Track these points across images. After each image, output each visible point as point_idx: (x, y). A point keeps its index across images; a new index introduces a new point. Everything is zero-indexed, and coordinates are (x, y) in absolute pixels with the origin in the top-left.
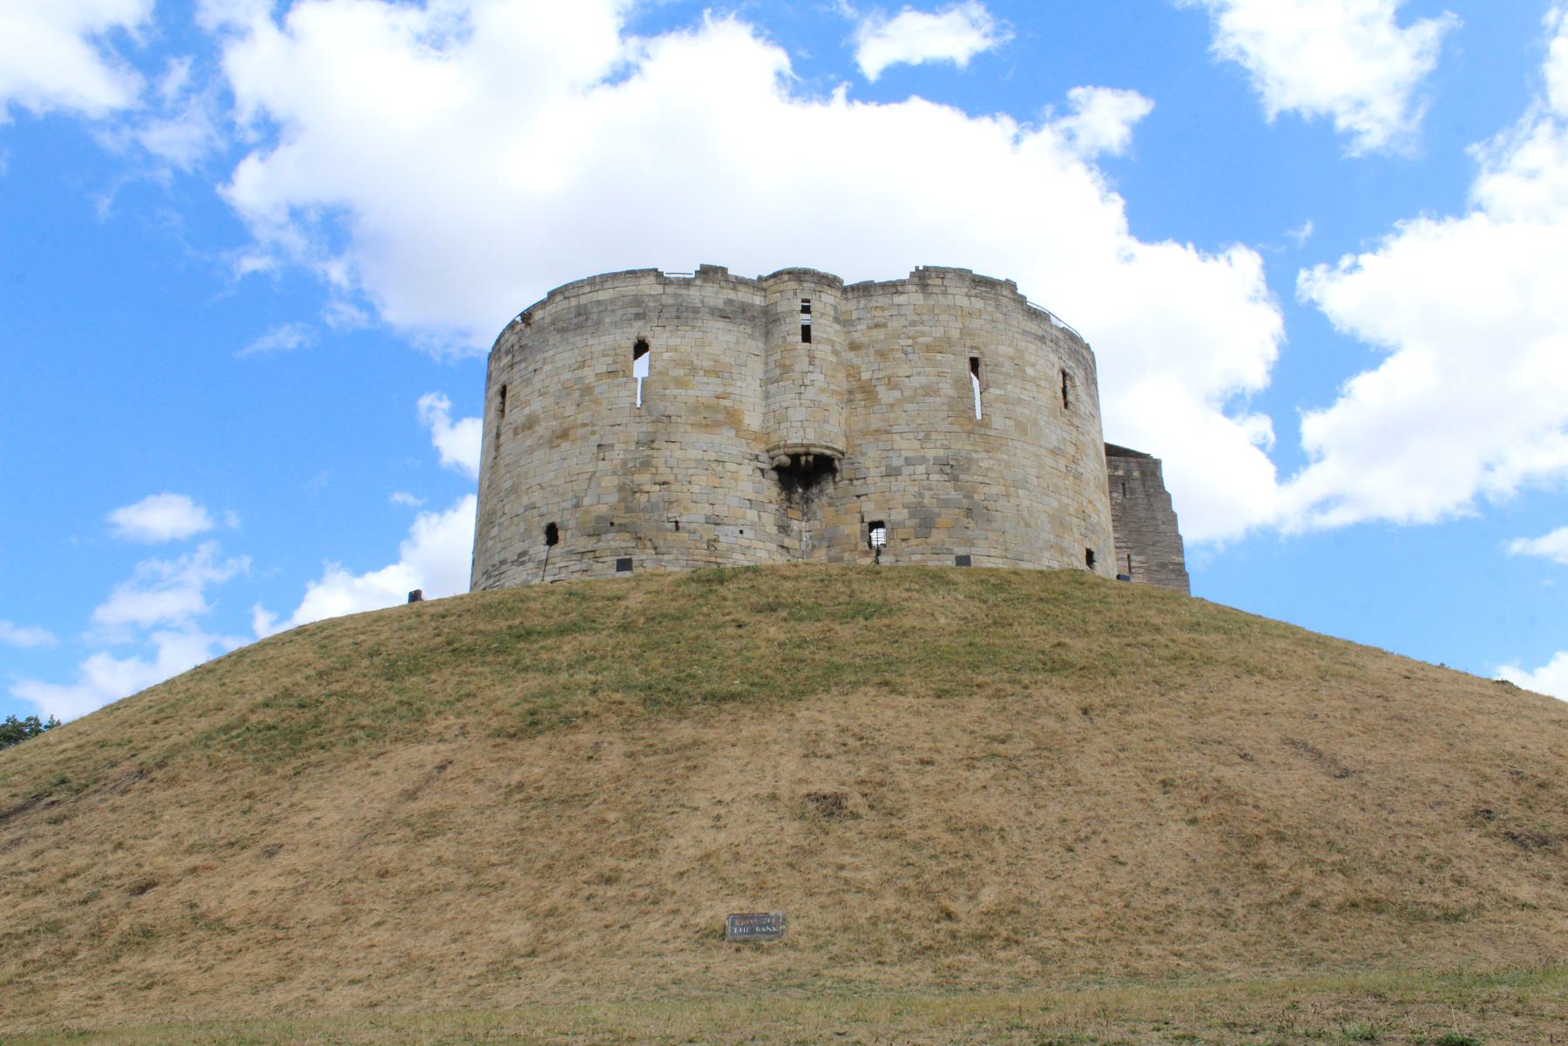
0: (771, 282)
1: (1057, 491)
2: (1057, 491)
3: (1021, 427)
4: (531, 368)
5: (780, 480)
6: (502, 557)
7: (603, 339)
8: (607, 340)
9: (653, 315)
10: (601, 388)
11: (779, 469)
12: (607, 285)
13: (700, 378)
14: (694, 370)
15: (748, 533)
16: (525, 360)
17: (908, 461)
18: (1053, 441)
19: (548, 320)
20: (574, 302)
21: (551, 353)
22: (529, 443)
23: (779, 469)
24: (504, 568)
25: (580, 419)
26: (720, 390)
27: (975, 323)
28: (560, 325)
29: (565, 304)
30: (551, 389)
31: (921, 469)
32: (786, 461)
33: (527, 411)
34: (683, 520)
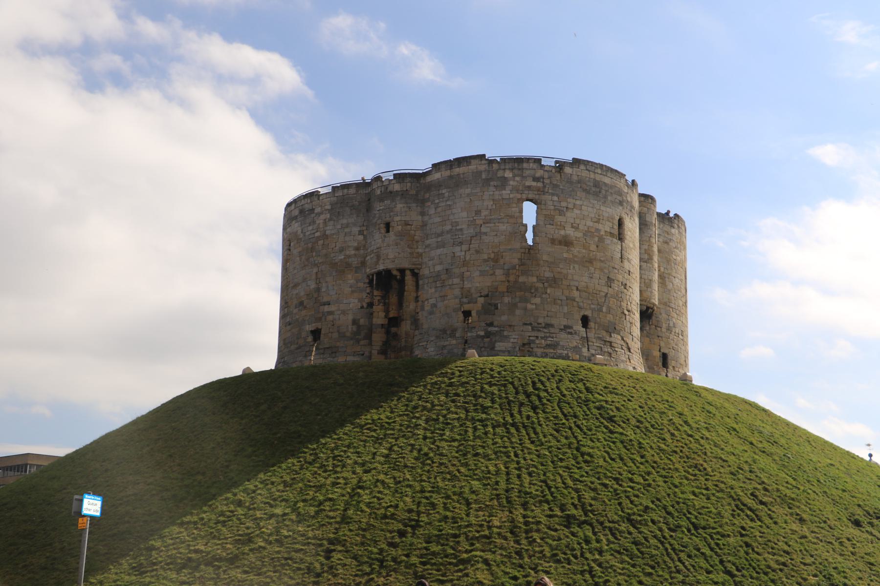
0: (642, 199)
4: (564, 204)
6: (548, 320)
7: (608, 209)
10: (608, 240)
12: (609, 174)
16: (557, 195)
19: (575, 178)
20: (592, 176)
21: (578, 202)
22: (565, 255)
24: (552, 330)
25: (599, 255)
28: (584, 186)
29: (585, 174)
30: (581, 227)
33: (562, 232)
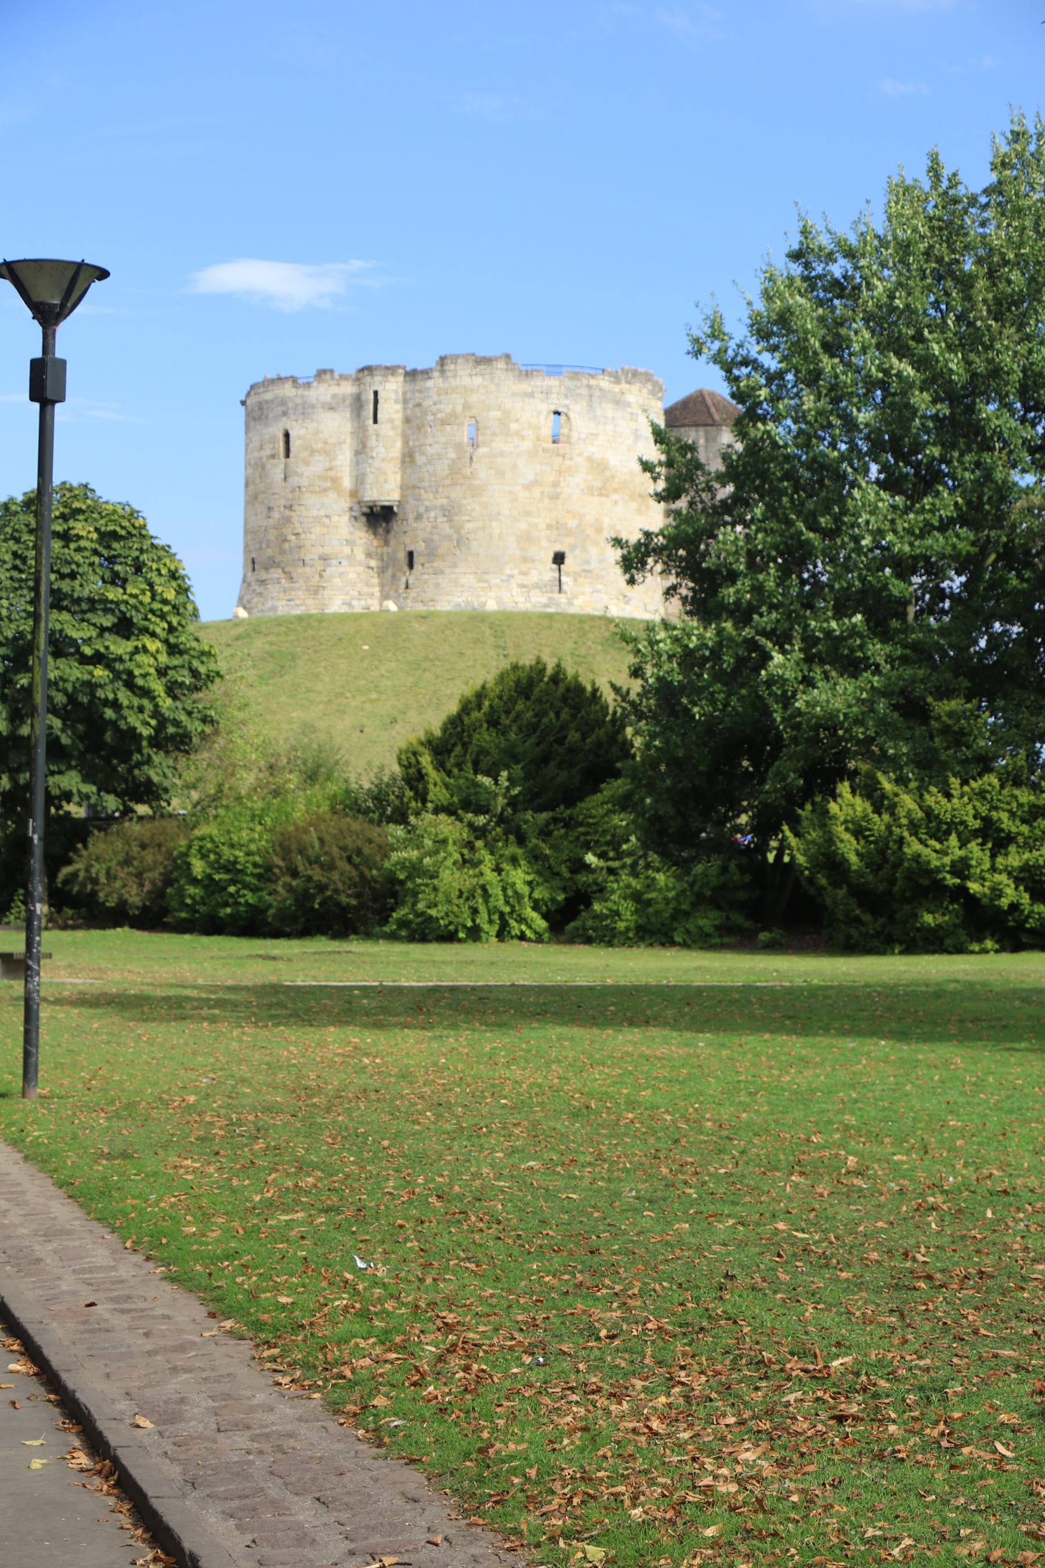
1: (528, 513)
2: (528, 513)
3: (501, 474)
5: (368, 521)
8: (270, 430)
9: (291, 412)
11: (364, 514)
13: (317, 457)
14: (313, 452)
15: (345, 563)
17: (427, 509)
18: (530, 477)
23: (364, 514)
26: (327, 465)
27: (473, 399)
31: (432, 514)
32: (366, 510)
34: (307, 558)
